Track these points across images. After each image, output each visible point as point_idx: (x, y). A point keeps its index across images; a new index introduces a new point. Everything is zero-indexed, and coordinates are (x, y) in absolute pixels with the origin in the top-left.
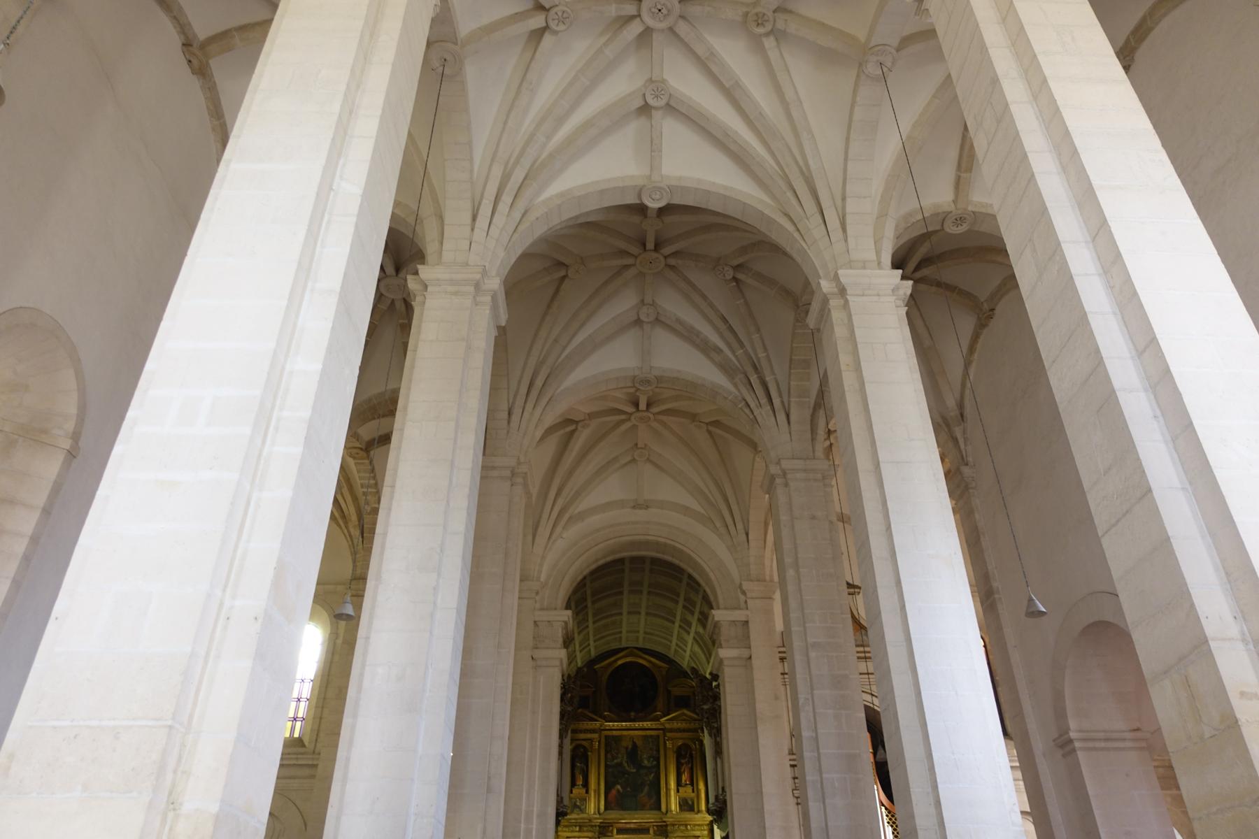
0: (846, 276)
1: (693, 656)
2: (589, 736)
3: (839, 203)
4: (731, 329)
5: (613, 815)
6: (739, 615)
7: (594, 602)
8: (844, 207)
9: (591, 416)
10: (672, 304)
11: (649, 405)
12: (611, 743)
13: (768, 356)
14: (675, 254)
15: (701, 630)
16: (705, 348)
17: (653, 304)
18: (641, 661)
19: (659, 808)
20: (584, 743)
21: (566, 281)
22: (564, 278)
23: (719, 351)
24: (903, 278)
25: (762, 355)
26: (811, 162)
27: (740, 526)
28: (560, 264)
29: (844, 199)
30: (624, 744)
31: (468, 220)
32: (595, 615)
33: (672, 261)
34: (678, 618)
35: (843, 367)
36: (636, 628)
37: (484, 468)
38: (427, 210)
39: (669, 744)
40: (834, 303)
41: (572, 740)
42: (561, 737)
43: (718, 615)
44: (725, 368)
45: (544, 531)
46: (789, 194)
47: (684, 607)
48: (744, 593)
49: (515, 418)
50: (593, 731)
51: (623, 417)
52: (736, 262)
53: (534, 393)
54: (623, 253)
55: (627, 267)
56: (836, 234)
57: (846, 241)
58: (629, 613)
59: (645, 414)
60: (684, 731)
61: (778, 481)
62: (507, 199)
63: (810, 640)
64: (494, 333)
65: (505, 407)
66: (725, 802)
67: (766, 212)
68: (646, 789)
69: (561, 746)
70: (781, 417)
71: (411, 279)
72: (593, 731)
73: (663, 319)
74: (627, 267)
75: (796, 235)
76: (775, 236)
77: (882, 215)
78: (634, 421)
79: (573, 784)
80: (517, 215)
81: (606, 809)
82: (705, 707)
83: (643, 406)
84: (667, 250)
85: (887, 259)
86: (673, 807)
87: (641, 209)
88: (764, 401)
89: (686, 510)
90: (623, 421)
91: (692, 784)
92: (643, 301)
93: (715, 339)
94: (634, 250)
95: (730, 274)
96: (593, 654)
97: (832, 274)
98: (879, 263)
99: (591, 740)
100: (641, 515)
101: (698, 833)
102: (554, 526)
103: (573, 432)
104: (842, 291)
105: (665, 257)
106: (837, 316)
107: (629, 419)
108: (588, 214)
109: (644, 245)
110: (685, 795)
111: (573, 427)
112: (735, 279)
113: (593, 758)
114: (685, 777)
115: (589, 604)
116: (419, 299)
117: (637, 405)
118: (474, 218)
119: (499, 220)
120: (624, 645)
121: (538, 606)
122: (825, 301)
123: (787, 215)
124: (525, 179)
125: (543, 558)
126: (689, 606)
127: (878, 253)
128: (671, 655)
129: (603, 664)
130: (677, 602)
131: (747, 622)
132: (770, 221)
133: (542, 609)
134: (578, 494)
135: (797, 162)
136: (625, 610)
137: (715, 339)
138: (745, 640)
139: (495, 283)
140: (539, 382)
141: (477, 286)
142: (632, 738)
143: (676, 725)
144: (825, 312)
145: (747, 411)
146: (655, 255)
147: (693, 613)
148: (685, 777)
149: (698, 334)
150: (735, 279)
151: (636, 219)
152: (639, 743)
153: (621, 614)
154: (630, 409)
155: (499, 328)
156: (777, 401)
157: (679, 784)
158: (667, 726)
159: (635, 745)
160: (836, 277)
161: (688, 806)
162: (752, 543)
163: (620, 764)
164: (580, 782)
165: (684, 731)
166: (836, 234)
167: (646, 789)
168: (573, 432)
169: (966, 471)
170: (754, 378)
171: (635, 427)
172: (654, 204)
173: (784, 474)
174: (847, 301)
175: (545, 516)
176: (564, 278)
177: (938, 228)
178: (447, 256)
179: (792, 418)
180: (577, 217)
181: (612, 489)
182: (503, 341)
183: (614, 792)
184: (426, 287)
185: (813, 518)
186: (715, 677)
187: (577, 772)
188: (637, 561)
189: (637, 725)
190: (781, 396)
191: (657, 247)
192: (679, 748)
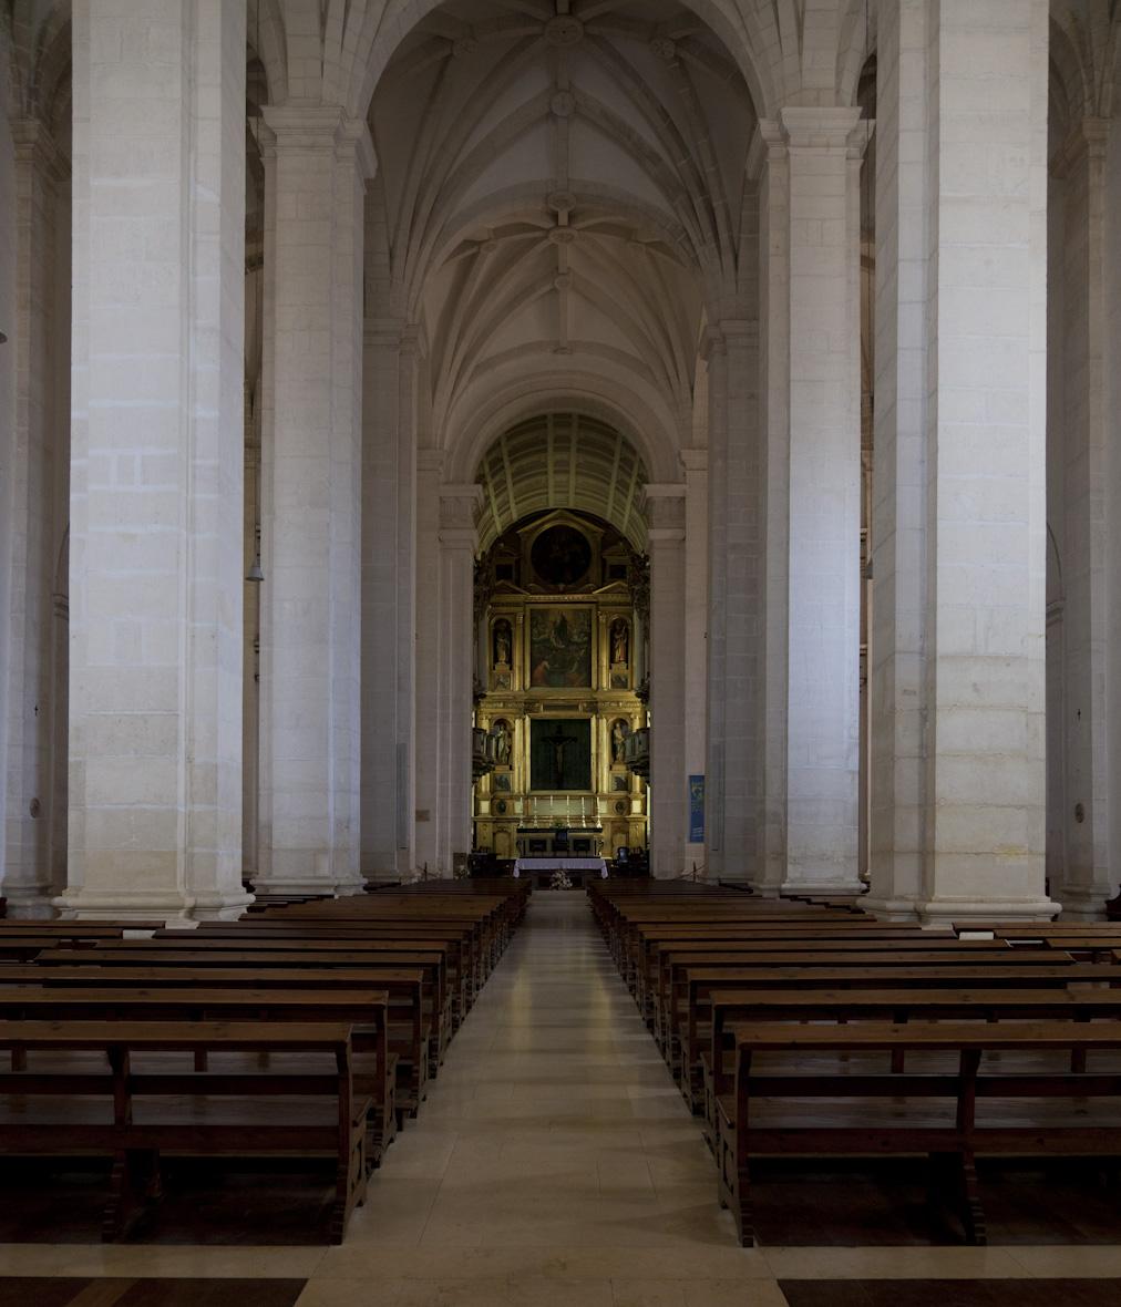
1: (632, 521)
2: (512, 609)
5: (540, 691)
6: (674, 490)
7: (511, 462)
10: (598, 88)
11: (571, 217)
12: (537, 618)
16: (640, 154)
18: (573, 525)
19: (590, 686)
20: (506, 617)
22: (450, 56)
30: (552, 618)
32: (513, 475)
34: (614, 479)
35: (772, 250)
36: (563, 489)
37: (366, 333)
39: (602, 619)
42: (477, 618)
45: (446, 386)
48: (683, 464)
50: (517, 604)
51: (538, 234)
53: (420, 226)
56: (790, 44)
57: (800, 54)
59: (569, 231)
60: (620, 604)
64: (362, 192)
68: (576, 665)
69: (476, 630)
70: (728, 259)
72: (517, 604)
78: (552, 239)
79: (496, 660)
81: (531, 686)
83: (563, 219)
86: (605, 685)
88: (709, 235)
90: (535, 241)
92: (556, 83)
96: (515, 517)
101: (630, 710)
102: (458, 377)
103: (474, 257)
104: (785, 137)
105: (584, 24)
106: (774, 172)
107: (546, 237)
110: (617, 672)
111: (474, 250)
112: (677, 58)
113: (517, 634)
114: (619, 654)
115: (507, 464)
117: (555, 217)
118: (323, 23)
119: (356, 20)
120: (551, 506)
122: (765, 149)
125: (446, 420)
126: (626, 465)
127: (839, 73)
128: (608, 519)
129: (526, 528)
130: (612, 462)
131: (683, 499)
133: (446, 483)
136: (551, 469)
139: (358, 128)
140: (425, 211)
141: (337, 135)
143: (611, 598)
147: (630, 476)
150: (677, 58)
152: (569, 618)
153: (546, 473)
154: (548, 224)
156: (724, 236)
157: (612, 660)
158: (601, 599)
159: (564, 620)
160: (778, 117)
161: (619, 683)
162: (698, 401)
163: (549, 639)
164: (503, 657)
165: (620, 604)
166: (790, 44)
167: (576, 665)
168: (474, 257)
170: (698, 201)
171: (554, 247)
173: (724, 338)
174: (788, 154)
175: (448, 358)
176: (450, 56)
179: (741, 259)
181: (526, 326)
182: (374, 195)
183: (540, 668)
184: (275, 137)
186: (647, 558)
188: (563, 419)
190: (730, 229)
192: (615, 622)
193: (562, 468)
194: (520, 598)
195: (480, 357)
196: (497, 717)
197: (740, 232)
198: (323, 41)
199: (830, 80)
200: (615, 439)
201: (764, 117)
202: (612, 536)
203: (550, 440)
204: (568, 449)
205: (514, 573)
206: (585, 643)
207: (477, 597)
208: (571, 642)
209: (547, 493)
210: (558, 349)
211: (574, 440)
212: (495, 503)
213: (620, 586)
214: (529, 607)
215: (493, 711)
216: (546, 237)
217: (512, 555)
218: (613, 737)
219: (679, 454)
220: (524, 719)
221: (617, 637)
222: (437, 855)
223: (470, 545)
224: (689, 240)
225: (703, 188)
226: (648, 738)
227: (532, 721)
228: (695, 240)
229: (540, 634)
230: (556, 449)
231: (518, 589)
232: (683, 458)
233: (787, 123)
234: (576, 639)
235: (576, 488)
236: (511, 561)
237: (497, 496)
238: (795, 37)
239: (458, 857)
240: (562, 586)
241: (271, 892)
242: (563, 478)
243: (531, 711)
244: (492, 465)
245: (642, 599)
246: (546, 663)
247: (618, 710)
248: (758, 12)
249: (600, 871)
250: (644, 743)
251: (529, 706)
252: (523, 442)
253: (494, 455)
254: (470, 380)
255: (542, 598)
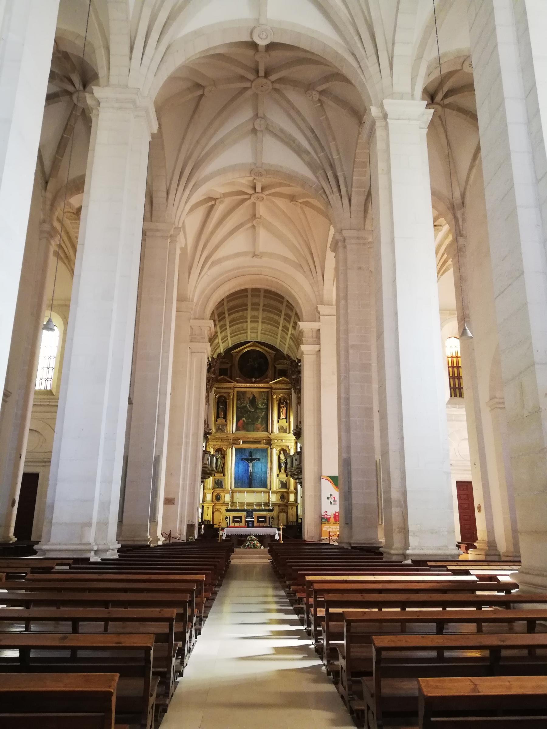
0: (389, 105)
1: (290, 347)
3: (390, 45)
4: (316, 137)
5: (242, 434)
8: (393, 51)
9: (225, 195)
10: (278, 118)
11: (263, 189)
12: (241, 395)
13: (340, 158)
14: (281, 80)
15: (293, 332)
16: (299, 151)
17: (264, 118)
19: (267, 431)
20: (224, 395)
21: (203, 98)
22: (202, 96)
23: (308, 153)
24: (428, 106)
25: (336, 157)
26: (373, 14)
27: (319, 271)
28: (199, 86)
29: (393, 44)
30: (248, 395)
31: (127, 50)
32: (230, 322)
33: (277, 86)
35: (380, 171)
36: (255, 331)
38: (97, 41)
40: (379, 124)
41: (216, 393)
42: (208, 391)
43: (302, 325)
44: (311, 165)
45: (196, 271)
46: (356, 38)
47: (284, 319)
48: (319, 313)
49: (171, 196)
50: (230, 388)
52: (320, 88)
54: (242, 78)
55: (246, 89)
57: (392, 77)
58: (251, 321)
59: (261, 195)
60: (283, 389)
61: (340, 244)
62: (155, 35)
63: (350, 343)
65: (165, 190)
66: (301, 429)
67: (340, 51)
68: (260, 420)
69: (207, 397)
70: (346, 201)
71: (88, 96)
72: (230, 388)
73: (271, 129)
74: (246, 89)
75: (359, 71)
76: (345, 71)
77: (419, 58)
78: (253, 199)
79: (218, 417)
80: (162, 48)
81: (237, 430)
82: (293, 377)
84: (274, 77)
85: (419, 91)
87: (253, 45)
88: (335, 190)
89: (285, 260)
91: (287, 419)
92: (257, 115)
93: (305, 144)
94: (251, 76)
95: (316, 96)
96: (230, 345)
97: (380, 102)
98: (413, 95)
99: (229, 393)
100: (257, 261)
101: (288, 444)
103: (212, 207)
104: (385, 116)
105: (272, 83)
106: (379, 133)
108: (216, 48)
109: (257, 72)
111: (213, 203)
112: (320, 100)
114: (283, 415)
115: (227, 315)
116: (94, 112)
117: (255, 188)
120: (249, 340)
121: (192, 317)
122: (374, 123)
123: (354, 55)
124: (168, 18)
125: (195, 287)
126: (288, 318)
127: (413, 88)
128: (277, 347)
130: (280, 316)
132: (343, 59)
133: (195, 319)
134: (217, 247)
135: (363, 12)
136: (249, 320)
137: (305, 144)
138: (317, 339)
140: (187, 172)
142: (252, 393)
143: (278, 386)
144: (372, 131)
145: (324, 196)
146: (264, 81)
148: (283, 415)
149: (294, 140)
151: (251, 52)
152: (256, 395)
153: (247, 322)
154: (251, 191)
155: (153, 136)
157: (279, 418)
158: (273, 386)
159: (254, 397)
160: (382, 106)
161: (282, 430)
163: (246, 406)
165: (283, 389)
167: (260, 420)
169: (461, 240)
170: (330, 174)
171: (254, 204)
172: (262, 42)
173: (344, 240)
174: (387, 124)
176: (202, 96)
177: (459, 68)
178: (113, 80)
179: (353, 202)
180: (208, 50)
181: (239, 243)
183: (241, 421)
184: (99, 103)
185: (360, 268)
186: (299, 361)
187: (220, 411)
188: (256, 291)
189: (256, 385)
190: (346, 186)
191: (266, 75)
192: (280, 399)
193: (255, 320)
194: (231, 385)
195: (215, 257)
196: (217, 447)
197: (352, 187)
198: (130, 59)
199: (408, 89)
200: (282, 303)
201: (372, 105)
202: (279, 354)
203: (249, 305)
204: (258, 309)
205: (229, 372)
206: (264, 409)
207: (208, 380)
208: (257, 408)
209: (247, 333)
210: (254, 255)
211: (261, 305)
212: (220, 336)
213: (283, 380)
214: (236, 390)
215: (215, 443)
216: (250, 198)
217: (228, 363)
218: (279, 459)
219: (317, 308)
220: (232, 448)
221: (282, 406)
222: (178, 526)
223: (204, 353)
224: (325, 192)
225: (332, 167)
226: (300, 457)
227: (236, 449)
228: (328, 192)
229: (241, 403)
230: (252, 309)
231: (230, 380)
232: (319, 309)
233: (386, 108)
234: (260, 406)
235: (261, 330)
236: (228, 366)
237: (221, 332)
238: (389, 68)
239: (190, 527)
240: (254, 379)
241: (47, 556)
242: (254, 325)
243: (236, 444)
244: (219, 315)
245: (296, 383)
246: (244, 419)
247: (282, 444)
248: (367, 58)
249: (274, 536)
250: (298, 460)
251: (235, 442)
252: (234, 305)
253: (220, 310)
254: (209, 269)
255: (243, 385)
